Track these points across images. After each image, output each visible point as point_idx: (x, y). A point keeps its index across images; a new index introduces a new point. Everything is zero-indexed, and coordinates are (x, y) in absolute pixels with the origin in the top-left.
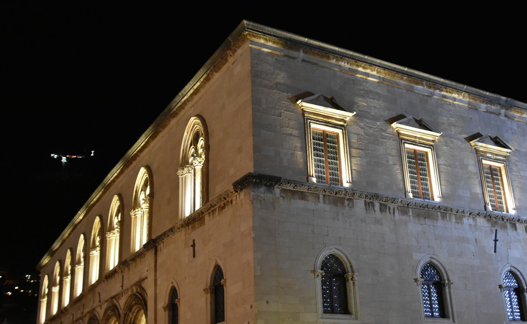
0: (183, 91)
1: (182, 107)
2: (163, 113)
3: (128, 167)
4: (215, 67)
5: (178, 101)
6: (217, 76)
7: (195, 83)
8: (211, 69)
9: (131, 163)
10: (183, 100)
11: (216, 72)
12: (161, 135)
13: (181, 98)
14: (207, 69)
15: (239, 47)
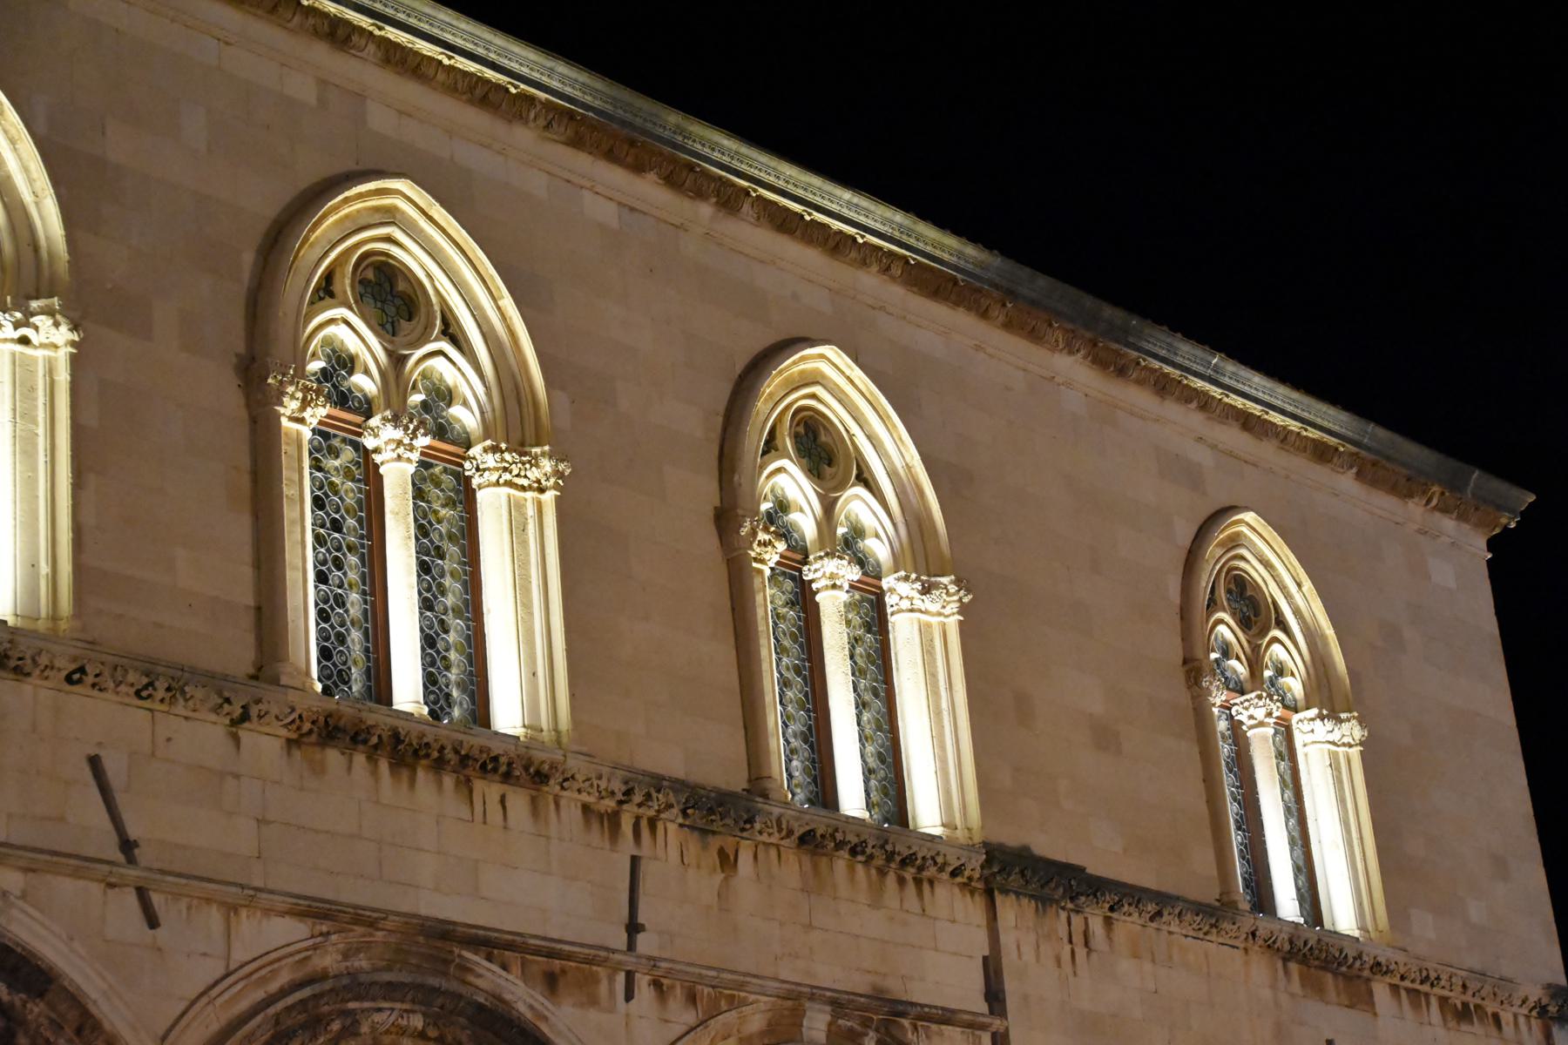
0: (1231, 367)
1: (1162, 387)
2: (1089, 301)
3: (576, 143)
4: (1374, 464)
5: (1179, 360)
6: (1346, 482)
7: (1290, 409)
8: (1363, 453)
9: (638, 168)
10: (1199, 384)
11: (1360, 476)
12: (961, 320)
13: (1200, 369)
14: (1356, 437)
15: (1462, 517)
